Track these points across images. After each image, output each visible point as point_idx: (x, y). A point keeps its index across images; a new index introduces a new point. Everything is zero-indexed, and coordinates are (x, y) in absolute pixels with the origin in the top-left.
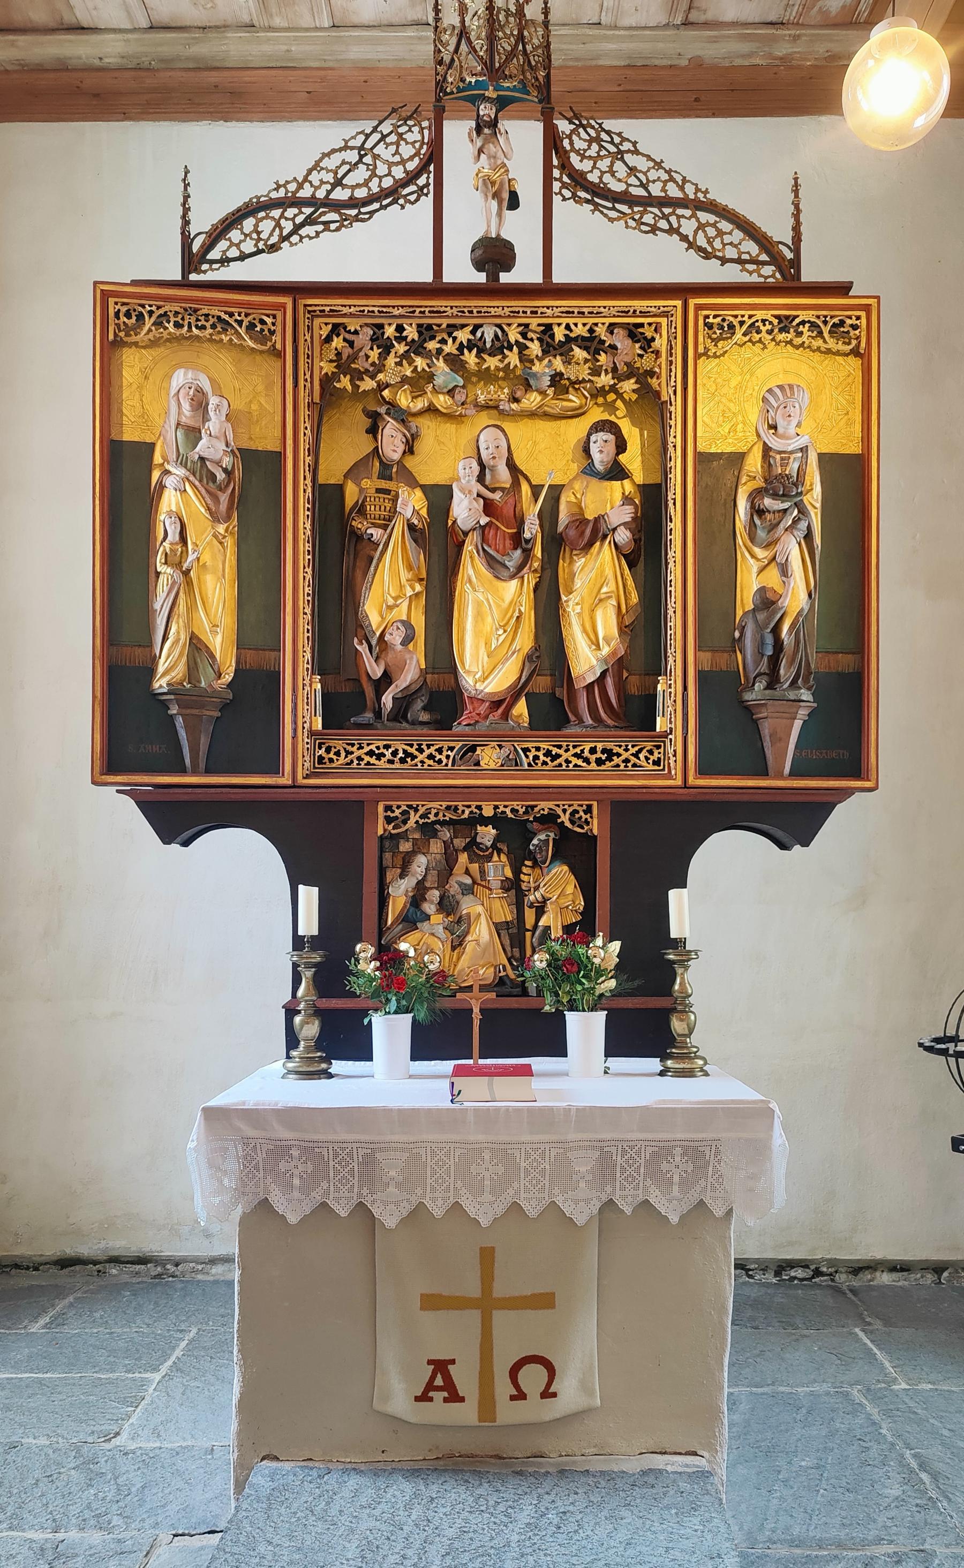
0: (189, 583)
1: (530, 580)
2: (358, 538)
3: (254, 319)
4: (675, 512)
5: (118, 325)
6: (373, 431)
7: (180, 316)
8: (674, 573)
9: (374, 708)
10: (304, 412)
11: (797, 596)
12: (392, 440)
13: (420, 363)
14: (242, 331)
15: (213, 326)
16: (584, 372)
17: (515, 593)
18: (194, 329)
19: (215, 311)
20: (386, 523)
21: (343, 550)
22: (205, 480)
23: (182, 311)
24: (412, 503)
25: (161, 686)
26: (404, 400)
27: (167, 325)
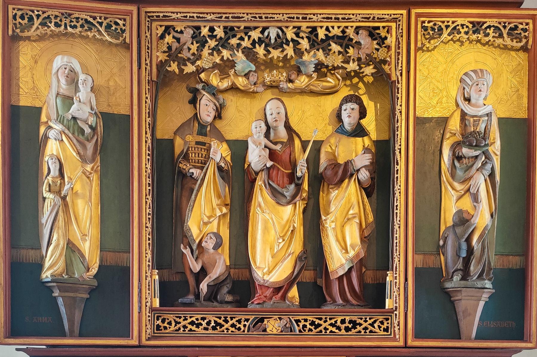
0: (66, 205)
1: (300, 205)
2: (183, 175)
3: (111, 21)
4: (401, 158)
5: (15, 24)
6: (194, 102)
7: (59, 19)
8: (399, 200)
9: (195, 292)
10: (145, 87)
11: (483, 218)
12: (206, 108)
13: (226, 53)
14: (102, 29)
15: (82, 26)
16: (338, 61)
17: (290, 214)
18: (68, 28)
19: (83, 16)
20: (202, 165)
21: (172, 183)
22: (76, 134)
23: (60, 15)
24: (220, 152)
25: (47, 277)
26: (215, 81)
27: (49, 25)
